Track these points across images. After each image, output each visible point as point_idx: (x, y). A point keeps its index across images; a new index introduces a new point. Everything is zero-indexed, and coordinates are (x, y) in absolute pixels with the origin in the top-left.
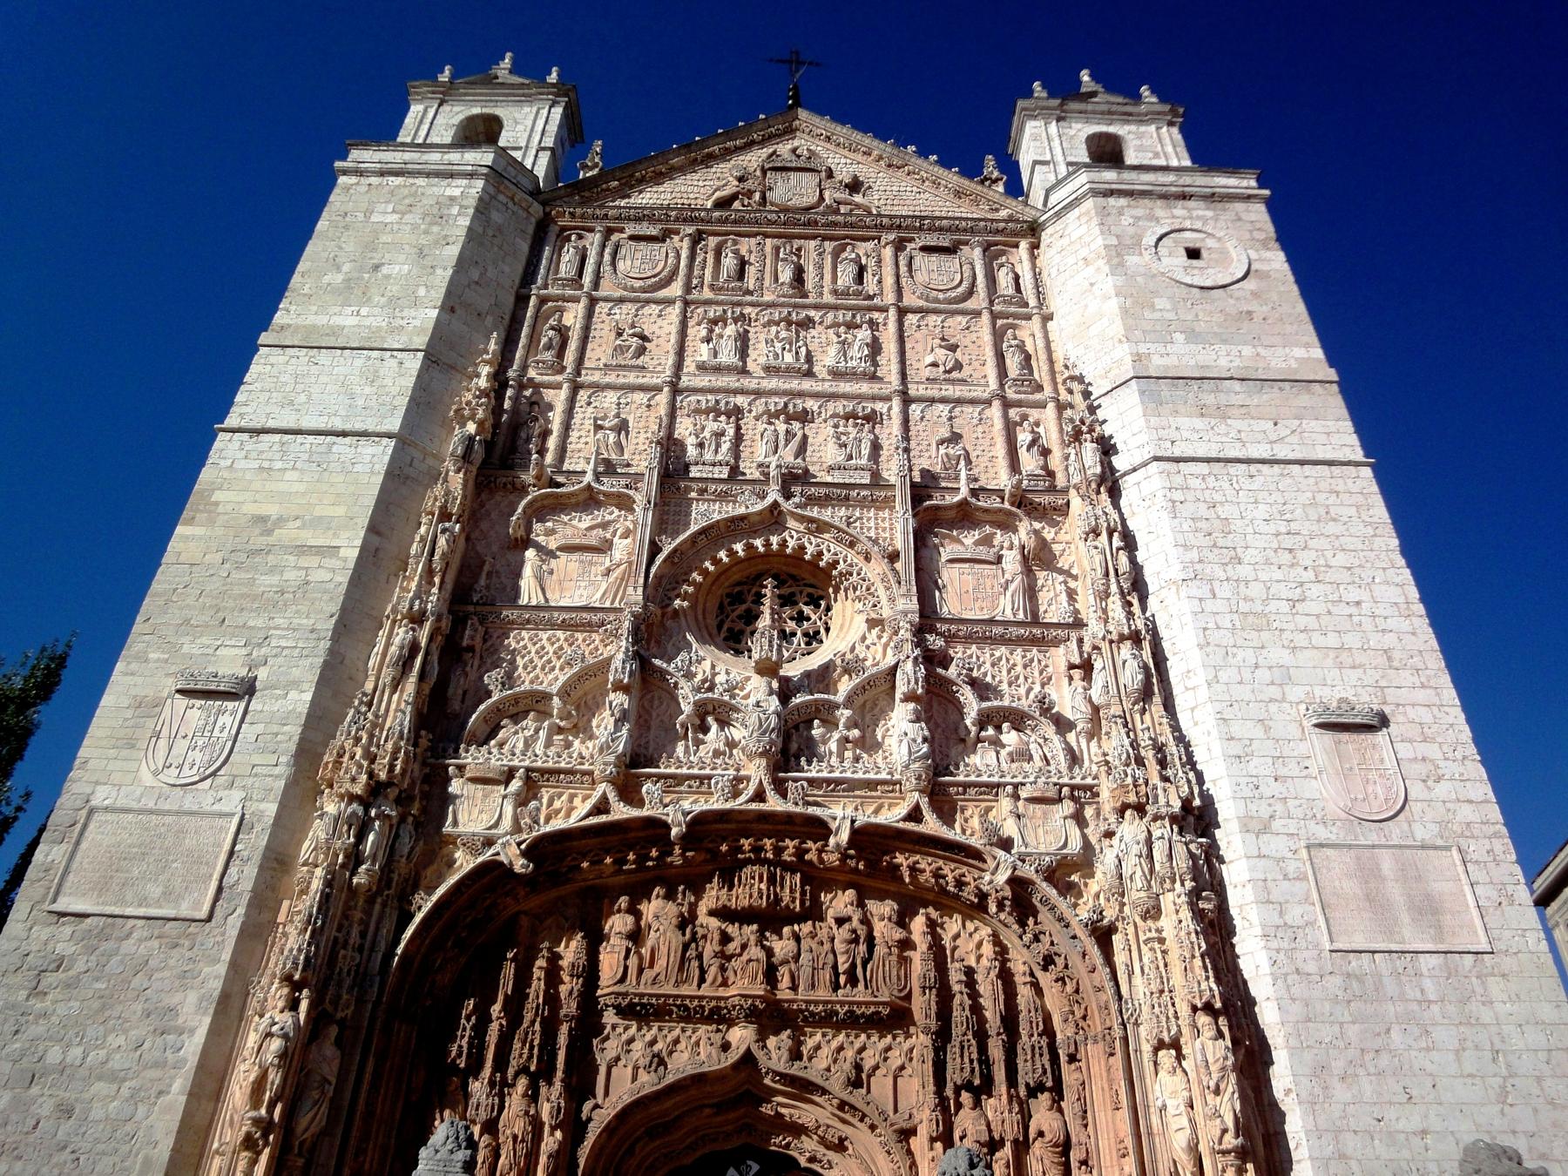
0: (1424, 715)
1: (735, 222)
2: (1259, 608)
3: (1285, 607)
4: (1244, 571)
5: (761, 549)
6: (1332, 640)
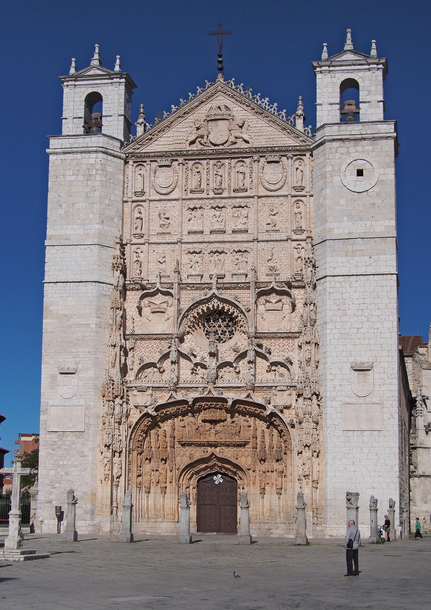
0: (386, 365)
1: (197, 155)
2: (347, 331)
3: (355, 330)
4: (346, 318)
5: (212, 309)
6: (367, 342)
